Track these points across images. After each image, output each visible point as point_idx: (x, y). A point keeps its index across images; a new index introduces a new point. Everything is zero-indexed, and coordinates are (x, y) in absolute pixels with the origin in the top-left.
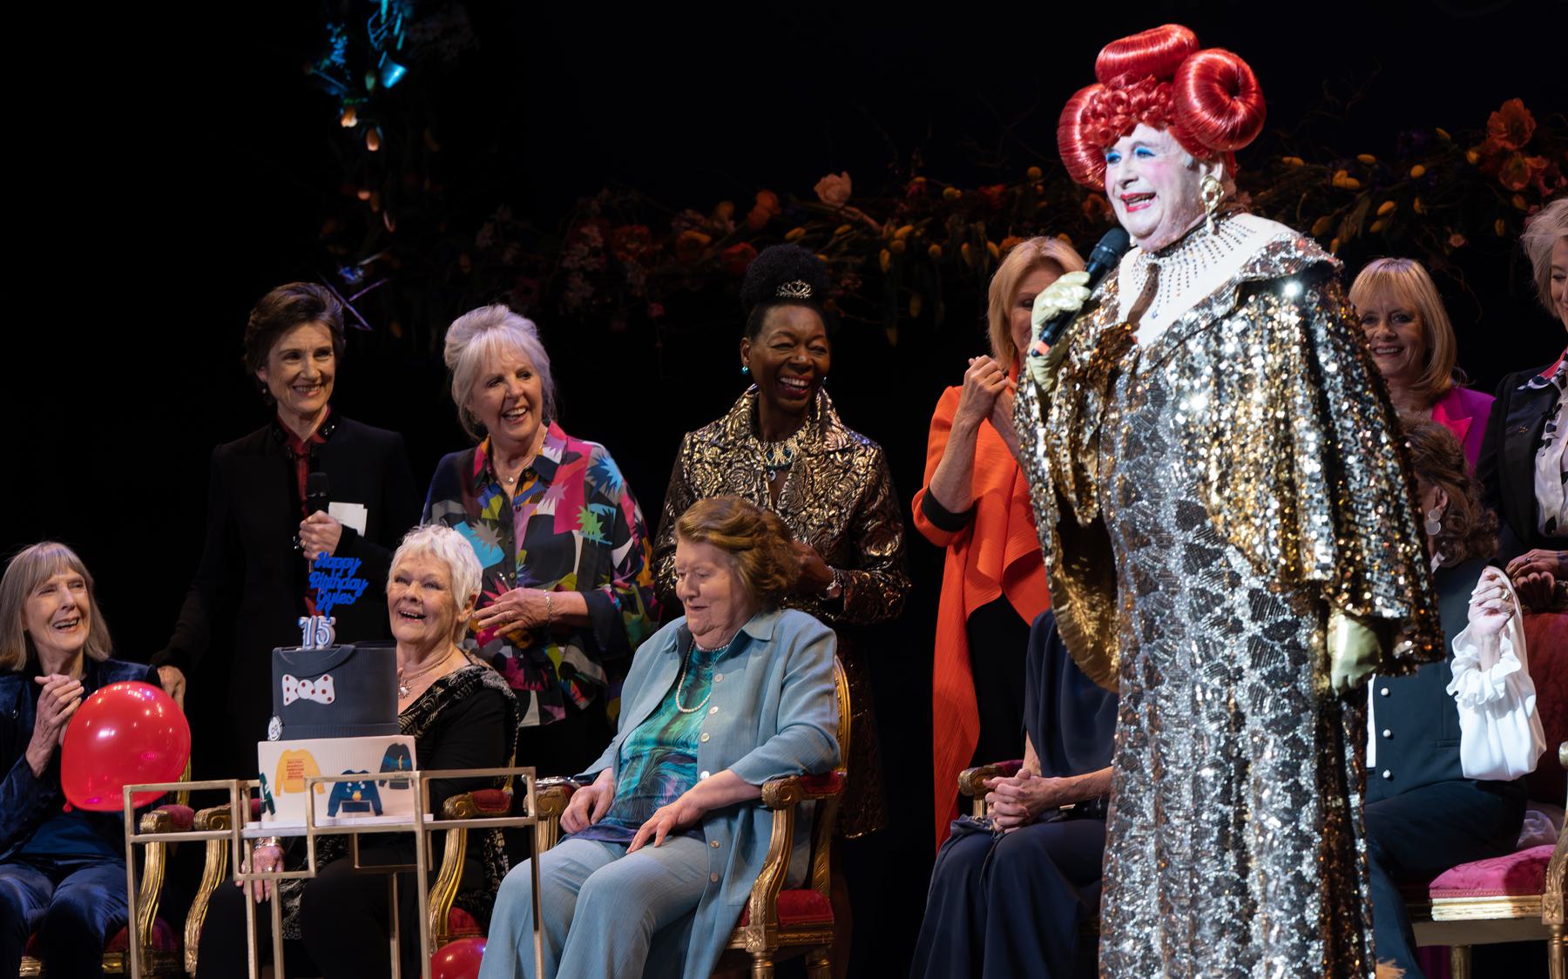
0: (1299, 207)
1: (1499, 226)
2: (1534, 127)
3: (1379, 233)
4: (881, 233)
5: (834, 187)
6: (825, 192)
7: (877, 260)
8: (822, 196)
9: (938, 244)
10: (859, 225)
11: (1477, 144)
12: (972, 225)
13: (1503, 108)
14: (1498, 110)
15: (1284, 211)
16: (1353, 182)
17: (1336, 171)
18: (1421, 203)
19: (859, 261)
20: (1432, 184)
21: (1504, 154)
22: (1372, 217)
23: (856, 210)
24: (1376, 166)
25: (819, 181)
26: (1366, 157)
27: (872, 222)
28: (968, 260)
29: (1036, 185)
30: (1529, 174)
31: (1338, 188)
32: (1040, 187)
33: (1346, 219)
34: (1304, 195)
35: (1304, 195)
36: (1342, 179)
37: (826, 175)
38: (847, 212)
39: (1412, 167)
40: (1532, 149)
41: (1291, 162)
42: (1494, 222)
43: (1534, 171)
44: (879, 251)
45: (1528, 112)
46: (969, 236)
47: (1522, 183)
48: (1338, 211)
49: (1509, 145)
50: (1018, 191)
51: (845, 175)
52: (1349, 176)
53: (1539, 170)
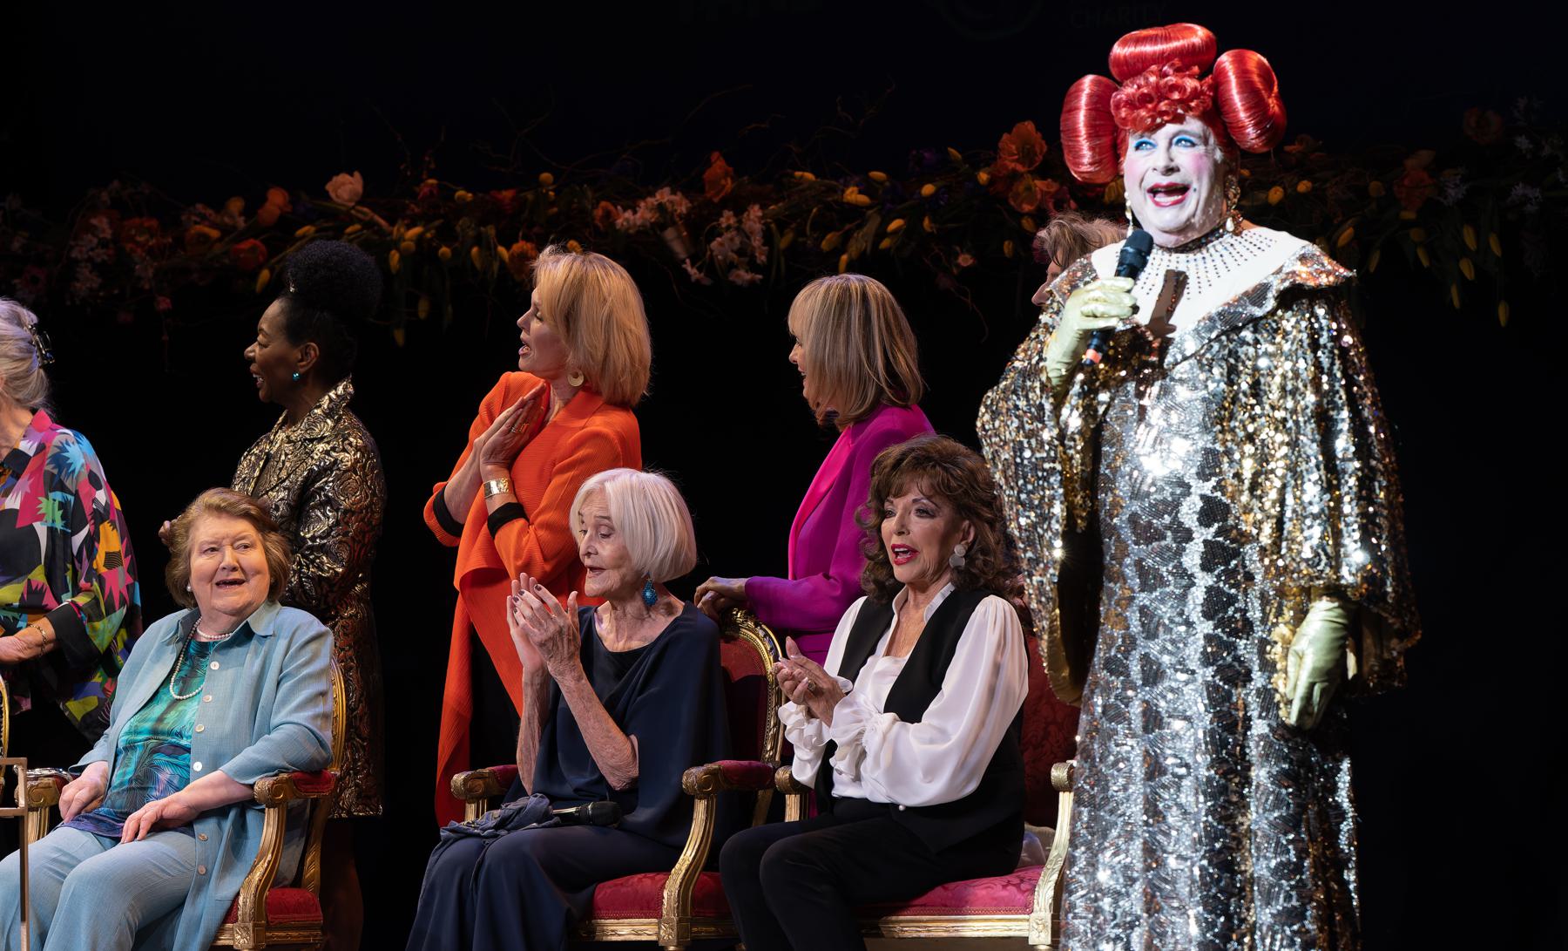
0: (809, 224)
1: (1008, 247)
2: (1045, 149)
3: (888, 250)
4: (391, 233)
5: (346, 187)
6: (336, 191)
8: (333, 195)
10: (369, 225)
11: (989, 165)
12: (482, 229)
14: (1010, 132)
15: (793, 226)
16: (863, 199)
17: (847, 186)
18: (931, 221)
21: (1015, 176)
22: (881, 234)
23: (365, 210)
24: (887, 184)
25: (330, 179)
26: (877, 175)
27: (382, 222)
28: (478, 265)
30: (1039, 196)
31: (849, 204)
32: (551, 193)
33: (855, 235)
34: (815, 210)
35: (815, 210)
36: (853, 195)
37: (338, 174)
38: (358, 211)
41: (802, 176)
42: (1003, 244)
45: (1039, 135)
46: (479, 240)
47: (1031, 204)
48: (847, 227)
49: (1020, 168)
50: (530, 196)
51: (357, 174)
52: (860, 192)
53: (1049, 192)
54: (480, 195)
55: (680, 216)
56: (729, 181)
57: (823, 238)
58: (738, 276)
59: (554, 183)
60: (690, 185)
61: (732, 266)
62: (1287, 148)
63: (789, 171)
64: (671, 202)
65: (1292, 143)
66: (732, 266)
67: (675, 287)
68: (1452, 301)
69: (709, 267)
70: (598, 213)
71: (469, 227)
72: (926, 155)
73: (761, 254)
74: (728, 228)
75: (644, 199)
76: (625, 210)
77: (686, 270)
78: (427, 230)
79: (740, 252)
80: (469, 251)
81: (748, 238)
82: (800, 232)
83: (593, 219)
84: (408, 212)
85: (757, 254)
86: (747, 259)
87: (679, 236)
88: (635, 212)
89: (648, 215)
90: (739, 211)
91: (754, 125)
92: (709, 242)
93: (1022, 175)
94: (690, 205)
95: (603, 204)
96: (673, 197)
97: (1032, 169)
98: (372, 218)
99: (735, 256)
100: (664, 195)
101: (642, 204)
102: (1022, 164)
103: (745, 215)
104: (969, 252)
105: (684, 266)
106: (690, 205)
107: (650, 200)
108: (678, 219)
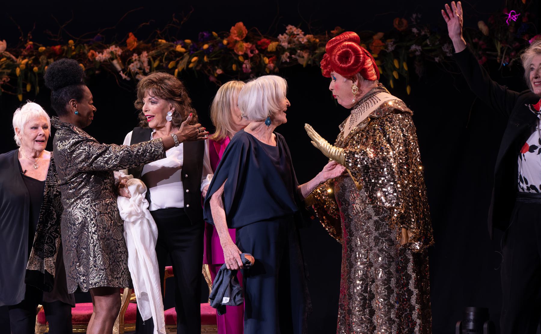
0: (164, 58)
1: (234, 67)
2: (247, 32)
3: (192, 68)
4: (16, 62)
7: (15, 71)
9: (37, 66)
10: (9, 58)
11: (227, 38)
12: (49, 60)
13: (236, 25)
14: (234, 26)
15: (159, 59)
17: (177, 44)
18: (208, 57)
19: (9, 71)
20: (211, 51)
21: (236, 42)
22: (189, 62)
23: (8, 53)
24: (191, 44)
26: (188, 41)
27: (14, 57)
29: (72, 46)
30: (245, 49)
31: (178, 52)
32: (73, 47)
33: (180, 62)
34: (166, 54)
35: (166, 54)
36: (179, 48)
38: (6, 54)
39: (203, 45)
40: (246, 40)
41: (161, 42)
42: (232, 66)
43: (246, 48)
44: (16, 68)
45: (244, 27)
47: (242, 51)
48: (178, 59)
49: (238, 39)
50: (65, 48)
51: (4, 41)
52: (182, 47)
53: (248, 48)
54: (48, 47)
55: (119, 56)
56: (136, 43)
57: (169, 63)
58: (139, 77)
59: (74, 43)
60: (122, 44)
61: (137, 73)
62: (332, 32)
63: (157, 39)
64: (116, 51)
65: (334, 30)
66: (137, 73)
67: (117, 80)
68: (390, 85)
69: (129, 74)
70: (90, 54)
71: (44, 59)
72: (205, 34)
73: (147, 69)
74: (136, 60)
75: (106, 49)
76: (99, 53)
77: (120, 75)
78: (29, 60)
79: (140, 69)
80: (44, 68)
81: (143, 64)
82: (161, 61)
83: (88, 57)
84: (23, 54)
85: (146, 69)
86: (142, 71)
87: (118, 63)
88: (102, 54)
89: (107, 55)
90: (139, 54)
91: (144, 24)
92: (129, 64)
93: (239, 41)
94: (122, 51)
95: (92, 51)
96: (116, 49)
97: (242, 39)
98: (10, 56)
99: (138, 70)
100: (113, 48)
101: (105, 51)
102: (239, 37)
103: (141, 55)
104: (220, 68)
105: (120, 73)
106: (122, 51)
107: (108, 50)
108: (118, 56)
